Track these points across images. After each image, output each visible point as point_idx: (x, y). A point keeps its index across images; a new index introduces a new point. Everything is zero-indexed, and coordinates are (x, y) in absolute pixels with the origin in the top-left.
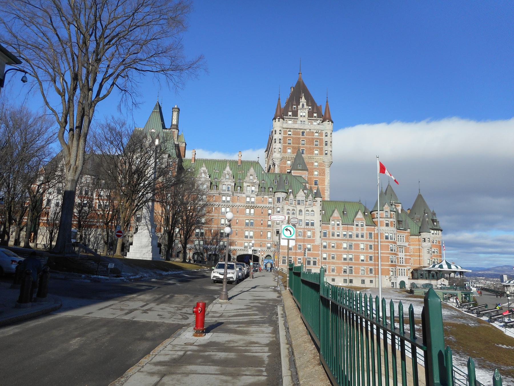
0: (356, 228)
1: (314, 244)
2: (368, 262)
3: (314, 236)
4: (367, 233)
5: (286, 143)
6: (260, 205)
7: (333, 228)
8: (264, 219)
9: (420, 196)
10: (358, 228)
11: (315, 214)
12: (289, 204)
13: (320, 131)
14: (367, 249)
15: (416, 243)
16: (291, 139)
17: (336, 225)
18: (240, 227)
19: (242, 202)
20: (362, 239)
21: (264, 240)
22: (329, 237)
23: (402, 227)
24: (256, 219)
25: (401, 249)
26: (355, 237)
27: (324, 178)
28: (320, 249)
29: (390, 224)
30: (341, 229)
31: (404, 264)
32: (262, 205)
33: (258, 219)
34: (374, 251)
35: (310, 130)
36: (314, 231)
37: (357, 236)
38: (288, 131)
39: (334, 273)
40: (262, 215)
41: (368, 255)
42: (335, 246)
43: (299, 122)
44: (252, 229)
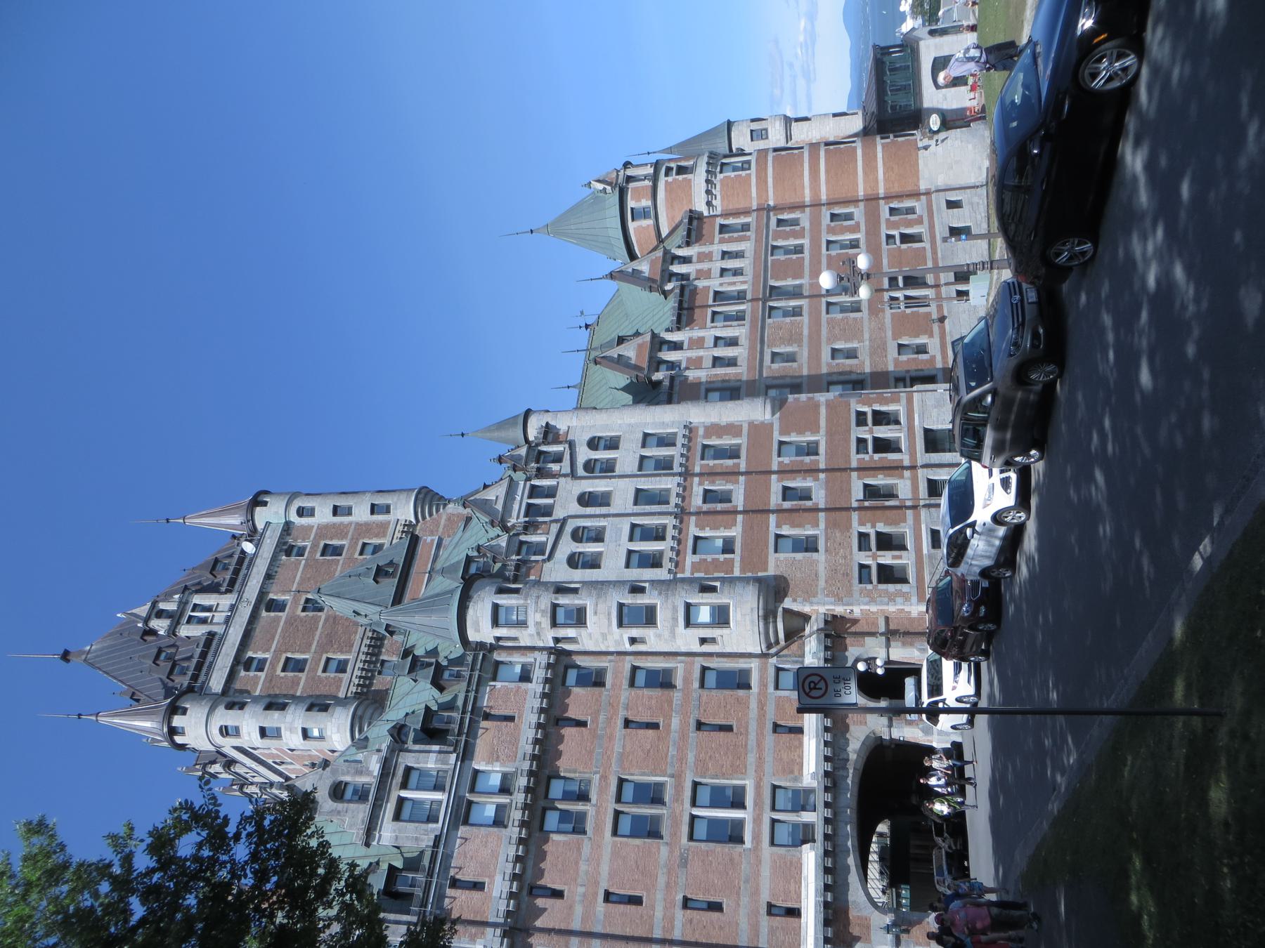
1: (776, 427)
3: (733, 429)
7: (696, 363)
8: (622, 714)
12: (539, 558)
18: (662, 880)
19: (495, 855)
21: (753, 705)
24: (614, 760)
26: (740, 278)
32: (529, 720)
33: (618, 748)
36: (701, 431)
37: (737, 272)
40: (595, 720)
44: (678, 788)
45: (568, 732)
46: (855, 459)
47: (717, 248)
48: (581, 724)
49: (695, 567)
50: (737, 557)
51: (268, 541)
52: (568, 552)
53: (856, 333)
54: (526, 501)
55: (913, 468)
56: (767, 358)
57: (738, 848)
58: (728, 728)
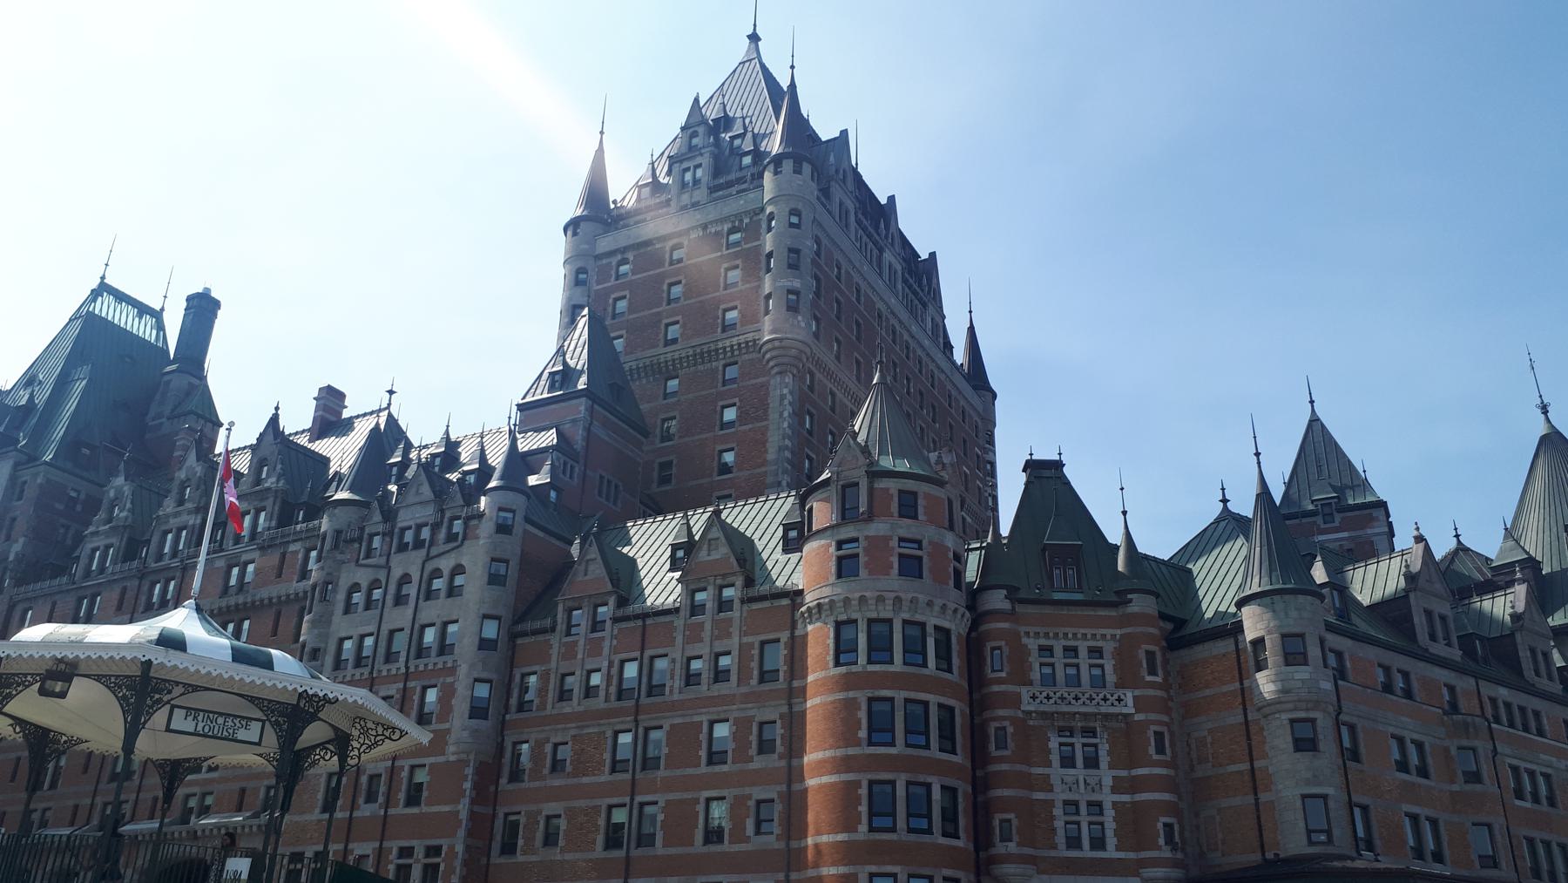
1: (441, 759)
2: (747, 840)
6: (264, 593)
7: (569, 653)
13: (746, 220)
15: (1225, 689)
16: (627, 293)
22: (543, 706)
23: (1080, 589)
25: (1078, 741)
29: (862, 559)
31: (1111, 852)
34: (783, 763)
36: (449, 680)
38: (614, 264)
41: (747, 790)
46: (394, 846)
51: (742, 202)
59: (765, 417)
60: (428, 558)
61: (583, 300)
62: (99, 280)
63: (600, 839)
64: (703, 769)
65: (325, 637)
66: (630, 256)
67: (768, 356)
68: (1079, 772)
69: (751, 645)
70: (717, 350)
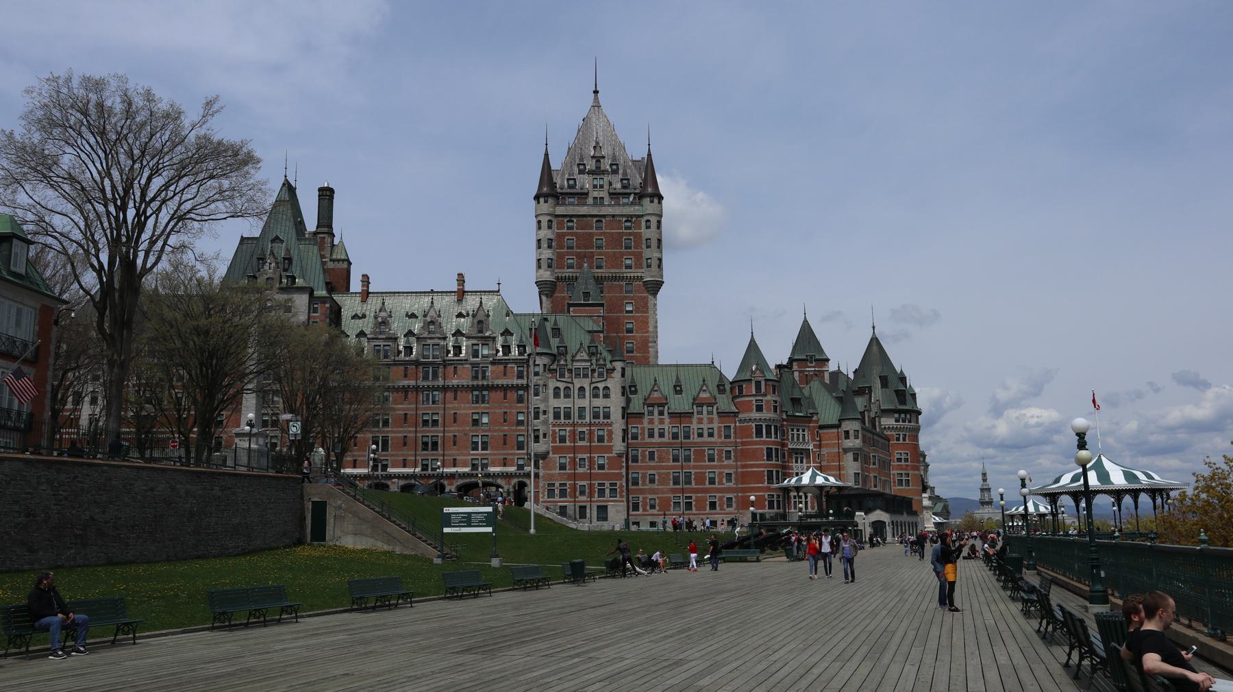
0: (698, 419)
1: (611, 455)
2: (724, 484)
3: (610, 439)
4: (720, 428)
5: (562, 247)
6: (500, 382)
7: (651, 422)
8: (508, 411)
9: (875, 342)
10: (702, 419)
11: (612, 395)
12: (558, 376)
14: (720, 459)
15: (833, 442)
17: (656, 412)
18: (460, 429)
19: (463, 379)
20: (710, 439)
21: (512, 452)
22: (644, 439)
23: (801, 412)
26: (696, 436)
27: (647, 318)
28: (624, 464)
30: (667, 421)
32: (504, 382)
35: (613, 216)
37: (700, 435)
38: (566, 221)
39: (655, 512)
40: (506, 402)
42: (656, 458)
43: (590, 201)
44: (486, 431)
45: (502, 394)
46: (596, 482)
47: (715, 425)
48: (505, 398)
49: (554, 431)
50: (558, 444)
51: (632, 209)
52: (560, 387)
53: (661, 483)
54: (581, 367)
55: (591, 501)
56: (651, 450)
57: (470, 449)
58: (505, 443)
59: (647, 312)
60: (592, 383)
61: (551, 237)
62: (284, 178)
63: (671, 482)
64: (707, 463)
65: (547, 406)
66: (575, 220)
67: (649, 286)
68: (799, 464)
69: (721, 427)
70: (623, 277)
